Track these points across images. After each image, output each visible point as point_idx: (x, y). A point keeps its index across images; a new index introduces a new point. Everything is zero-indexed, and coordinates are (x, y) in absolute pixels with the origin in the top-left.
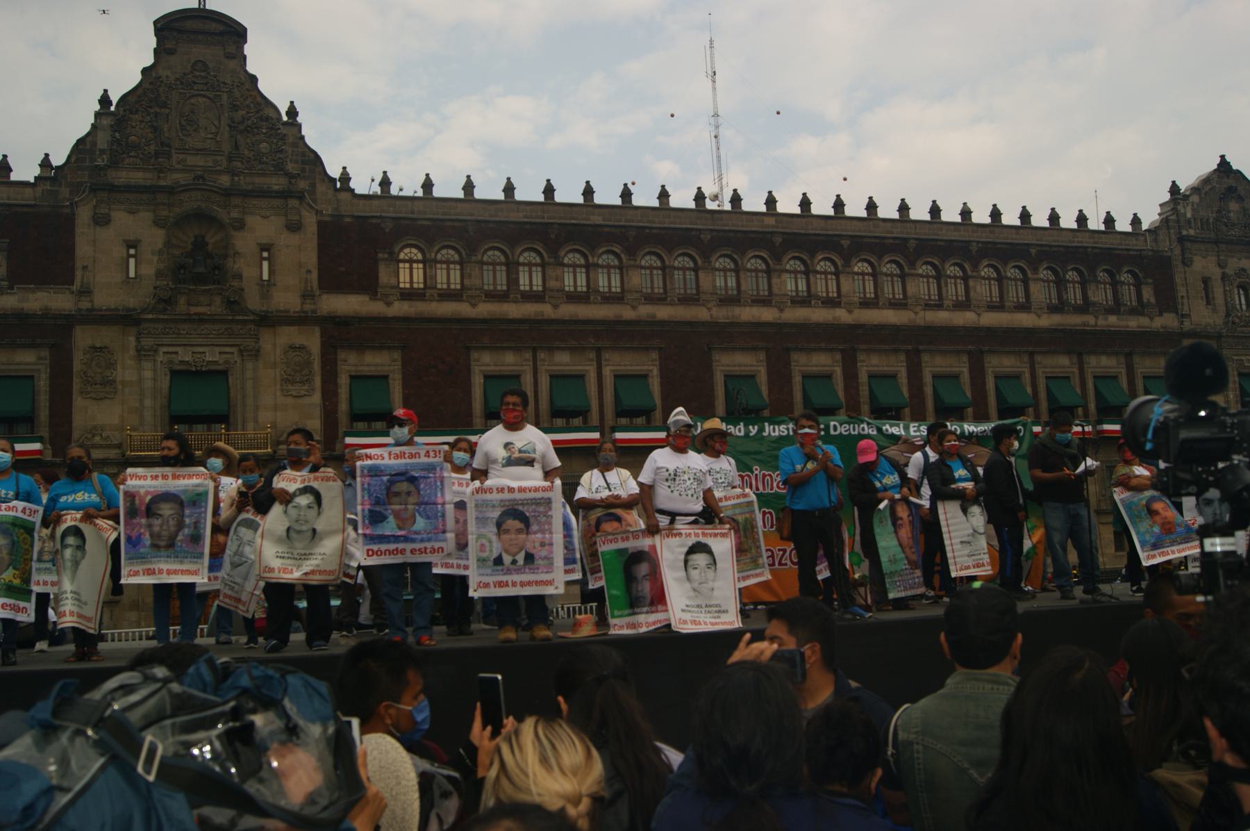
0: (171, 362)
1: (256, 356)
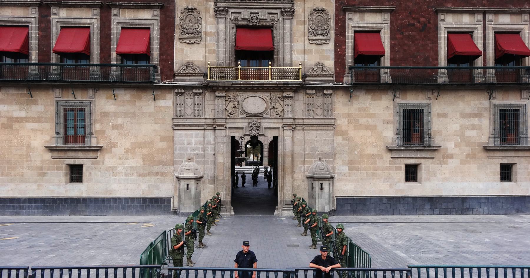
0: (236, 19)
1: (292, 16)
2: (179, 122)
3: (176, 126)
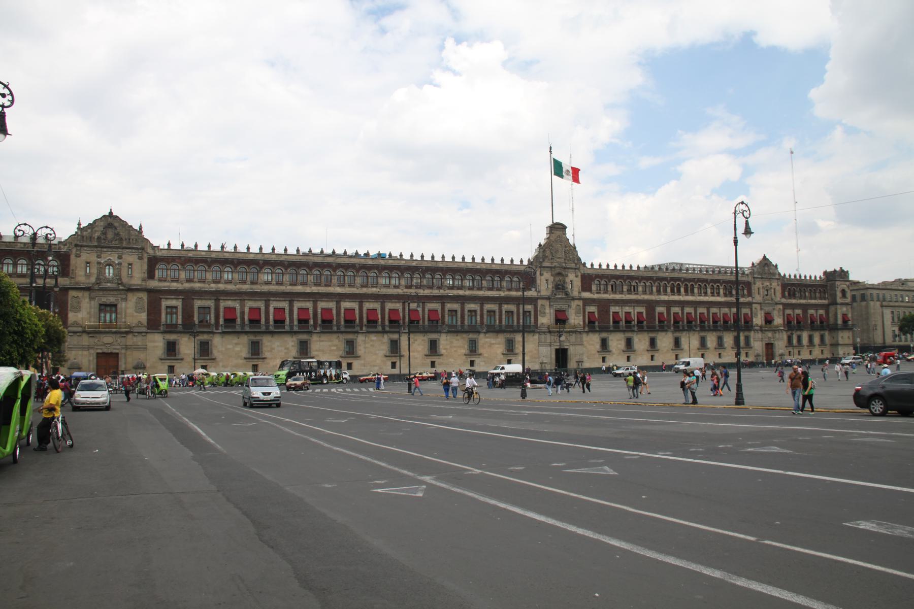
2: (540, 344)
3: (539, 345)
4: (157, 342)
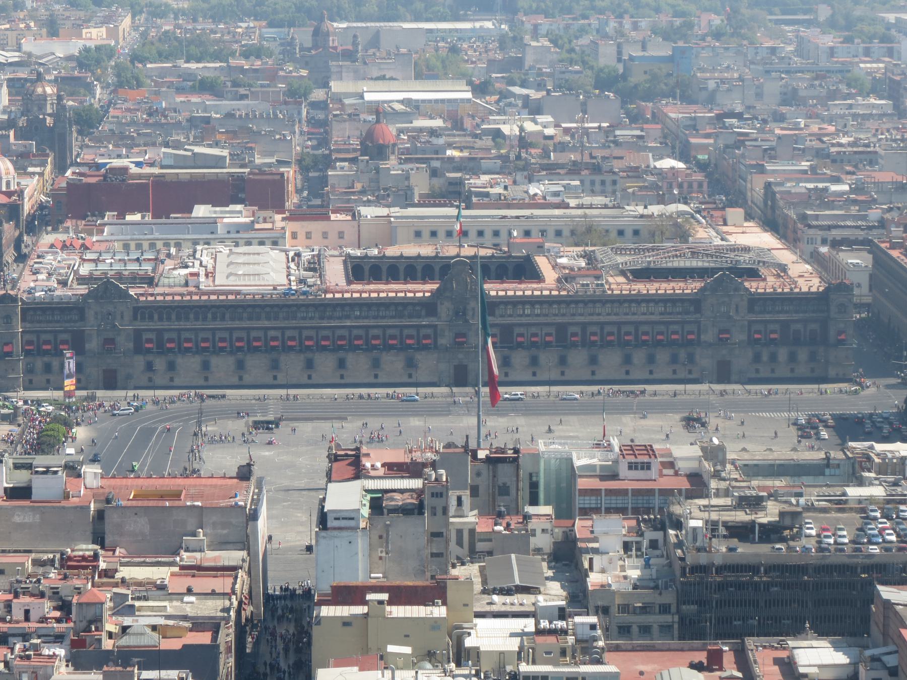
4: (140, 361)
